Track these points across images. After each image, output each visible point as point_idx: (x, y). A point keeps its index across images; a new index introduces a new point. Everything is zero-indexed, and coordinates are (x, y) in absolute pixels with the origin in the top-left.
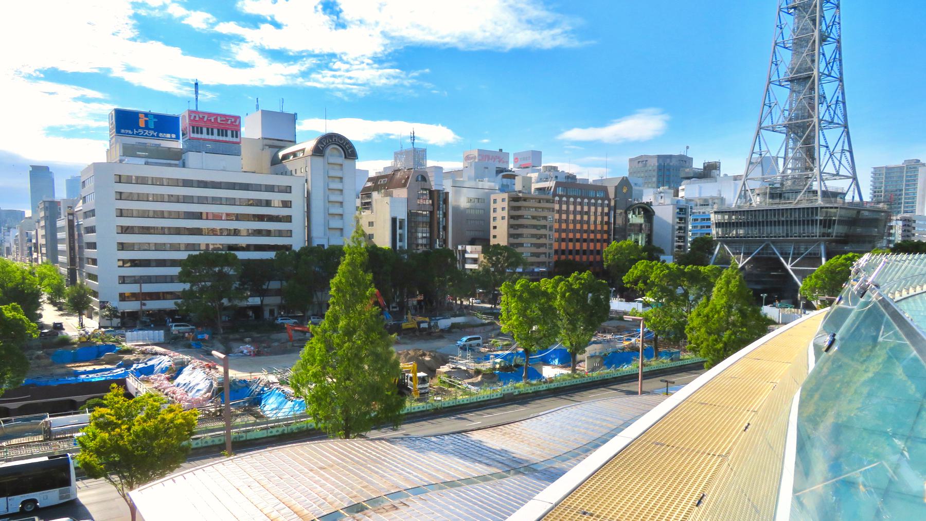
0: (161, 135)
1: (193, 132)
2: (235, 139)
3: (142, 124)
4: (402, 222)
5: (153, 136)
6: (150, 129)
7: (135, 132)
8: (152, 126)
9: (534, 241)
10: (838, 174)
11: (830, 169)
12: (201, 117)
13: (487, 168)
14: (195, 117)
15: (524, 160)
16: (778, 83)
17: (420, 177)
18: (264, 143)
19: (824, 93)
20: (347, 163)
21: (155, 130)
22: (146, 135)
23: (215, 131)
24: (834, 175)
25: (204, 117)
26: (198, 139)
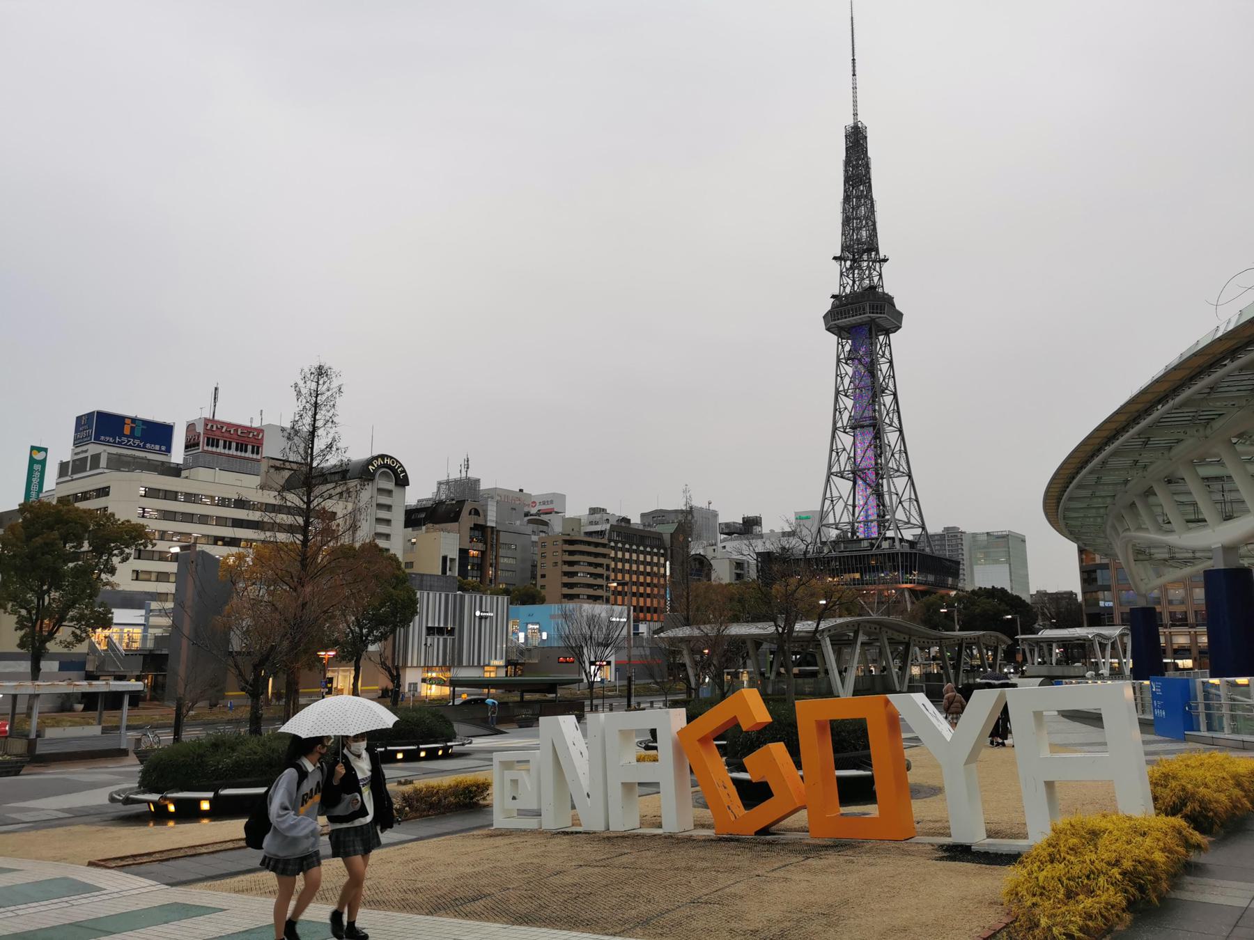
0: (148, 445)
1: (208, 445)
2: (255, 456)
3: (127, 431)
4: (452, 560)
5: (139, 446)
6: (135, 438)
7: (117, 439)
8: (138, 433)
9: (591, 592)
10: (909, 523)
11: (900, 515)
12: (219, 426)
13: (515, 509)
14: (212, 426)
15: (544, 504)
16: (842, 430)
17: (473, 511)
18: (270, 464)
19: (889, 442)
20: (396, 491)
21: (141, 439)
22: (130, 445)
23: (234, 445)
24: (906, 523)
25: (222, 427)
26: (213, 453)
